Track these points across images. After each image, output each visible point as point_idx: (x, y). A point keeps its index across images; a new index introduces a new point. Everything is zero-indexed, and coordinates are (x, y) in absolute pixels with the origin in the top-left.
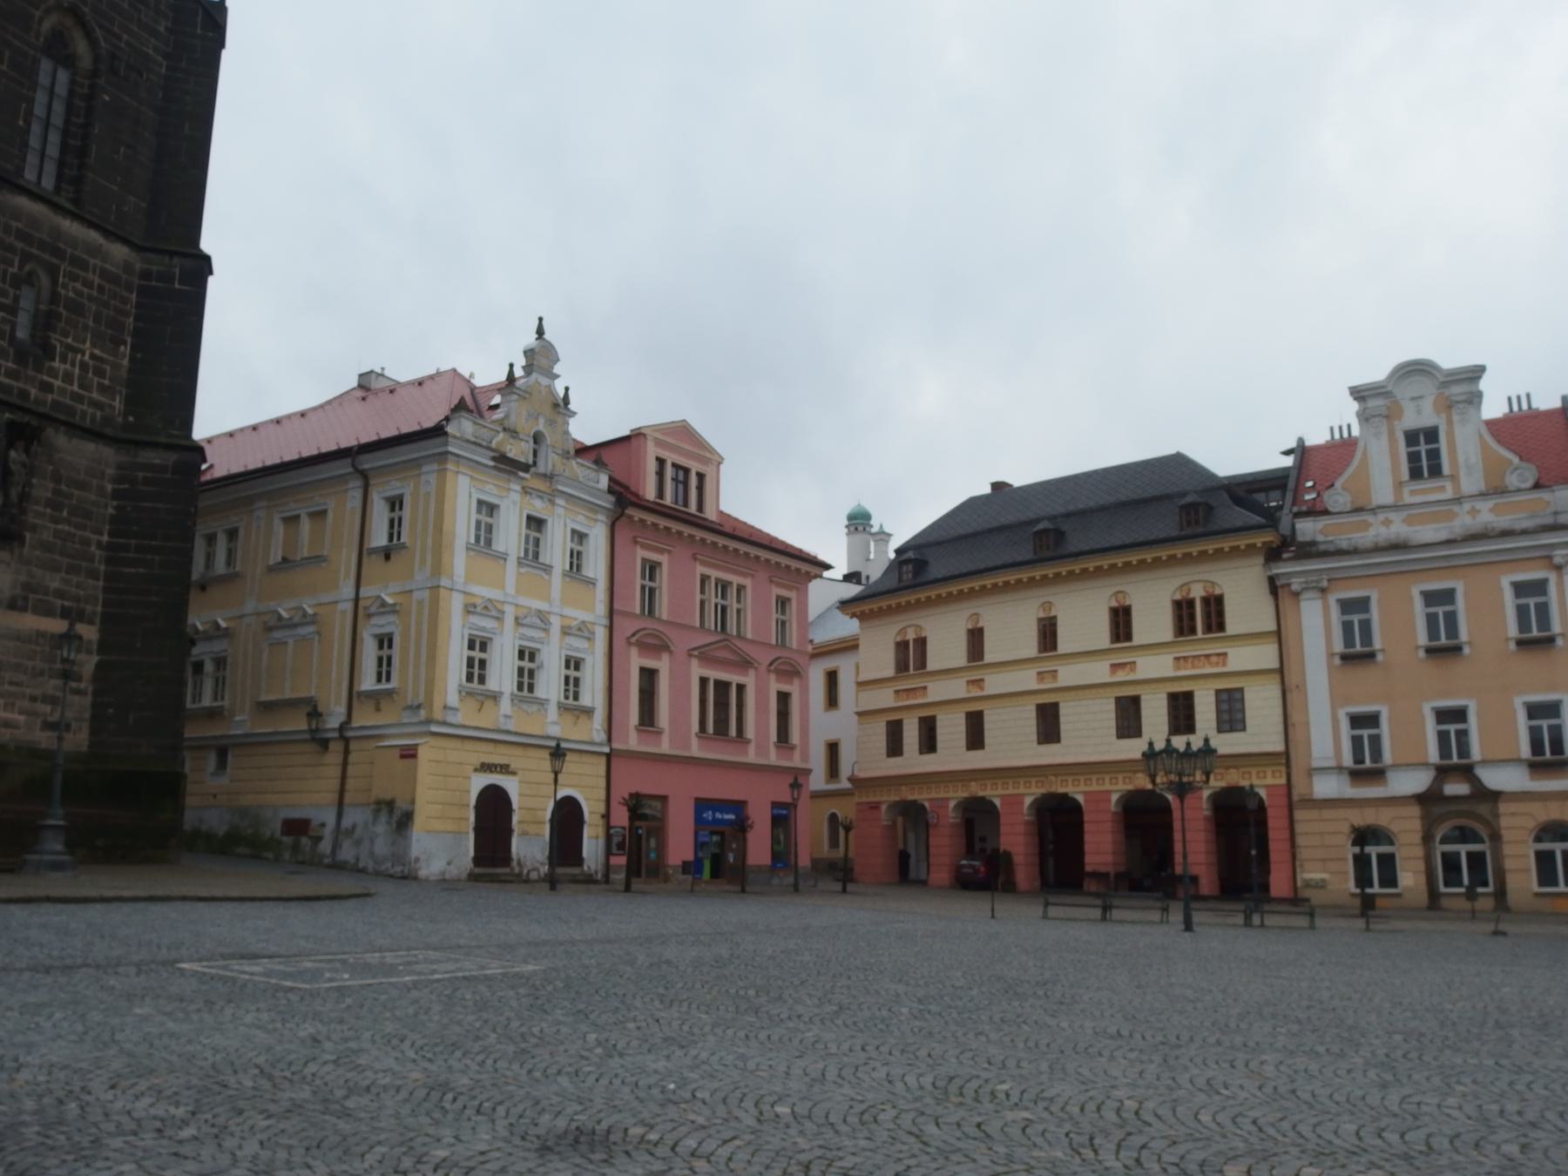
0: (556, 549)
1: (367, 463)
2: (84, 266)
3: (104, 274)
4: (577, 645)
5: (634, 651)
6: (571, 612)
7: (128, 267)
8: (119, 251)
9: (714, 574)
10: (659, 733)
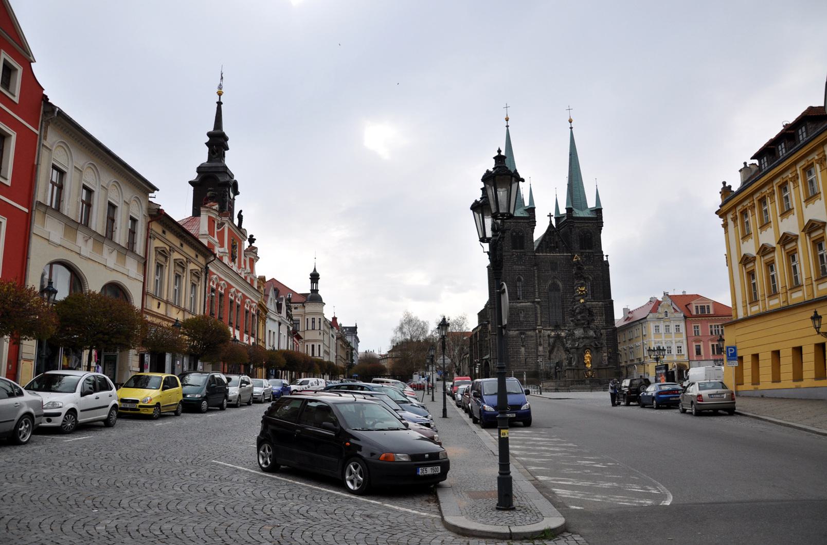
0: (673, 329)
1: (641, 321)
2: (596, 307)
3: (599, 307)
4: (679, 344)
5: (694, 343)
6: (676, 339)
7: (602, 305)
8: (601, 303)
9: (713, 324)
10: (702, 356)
